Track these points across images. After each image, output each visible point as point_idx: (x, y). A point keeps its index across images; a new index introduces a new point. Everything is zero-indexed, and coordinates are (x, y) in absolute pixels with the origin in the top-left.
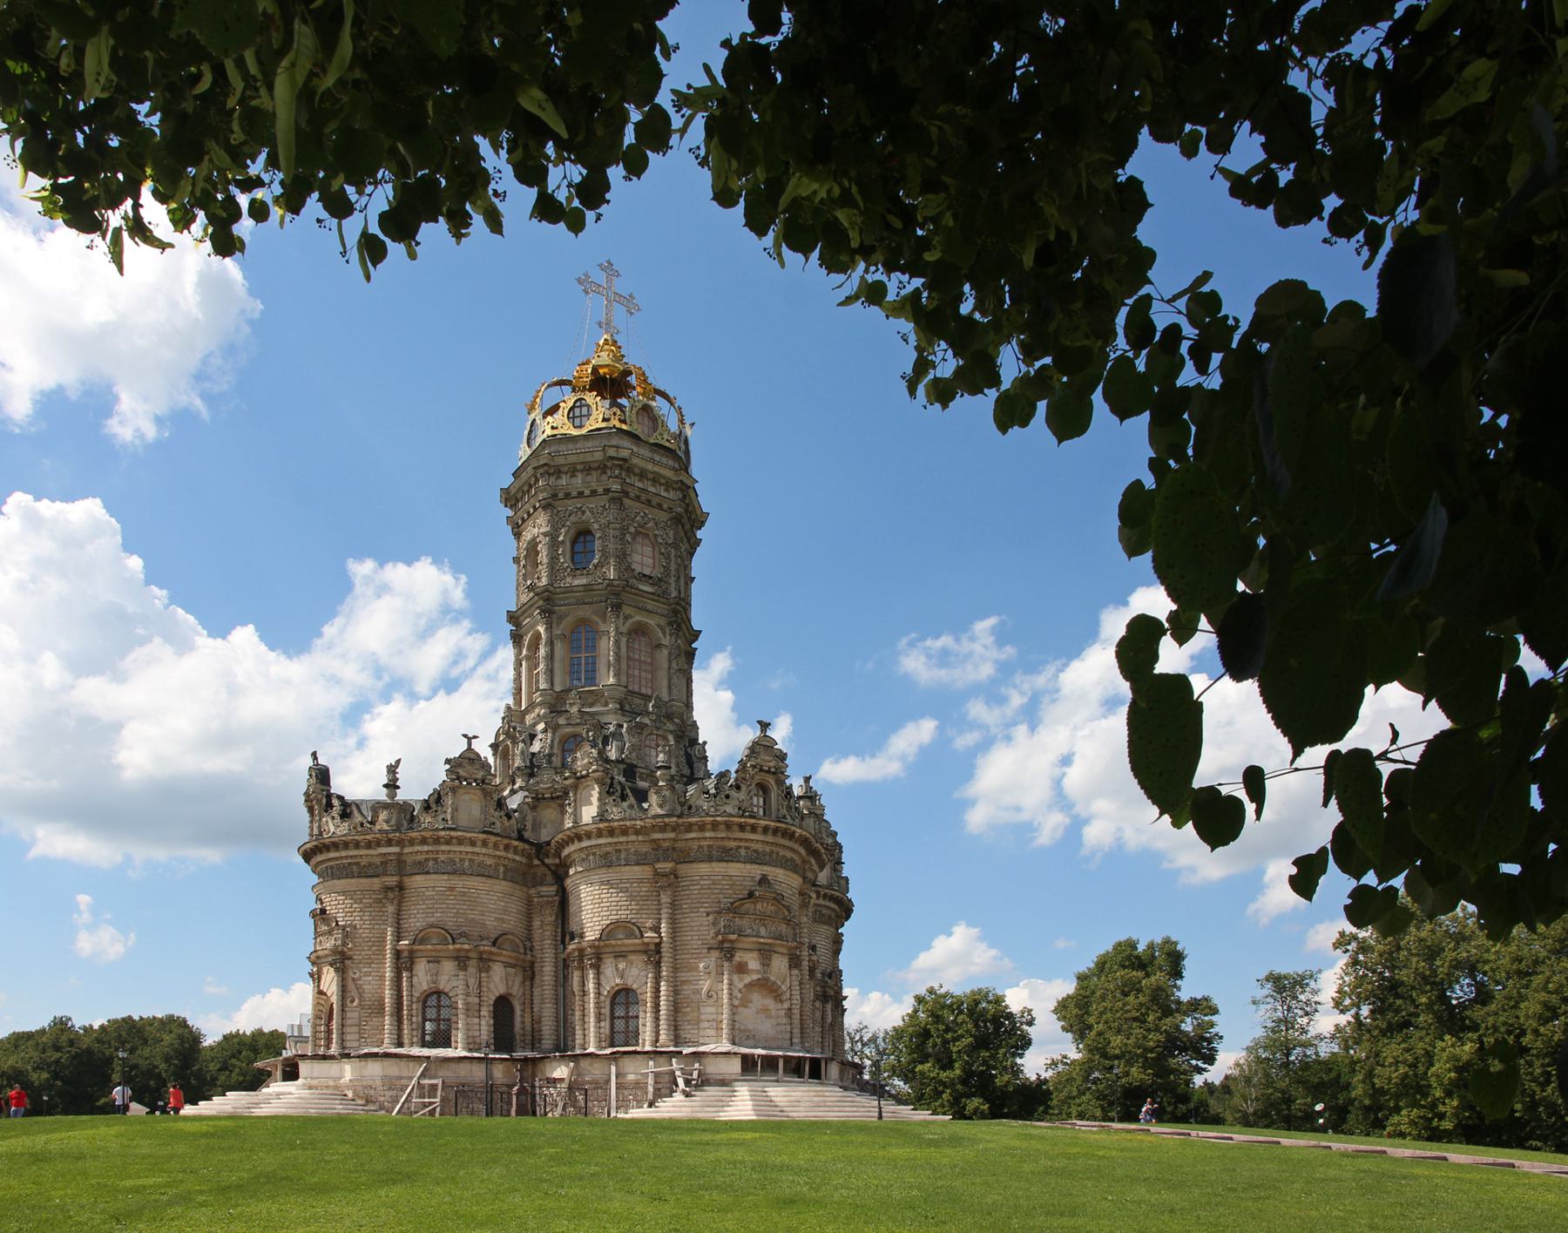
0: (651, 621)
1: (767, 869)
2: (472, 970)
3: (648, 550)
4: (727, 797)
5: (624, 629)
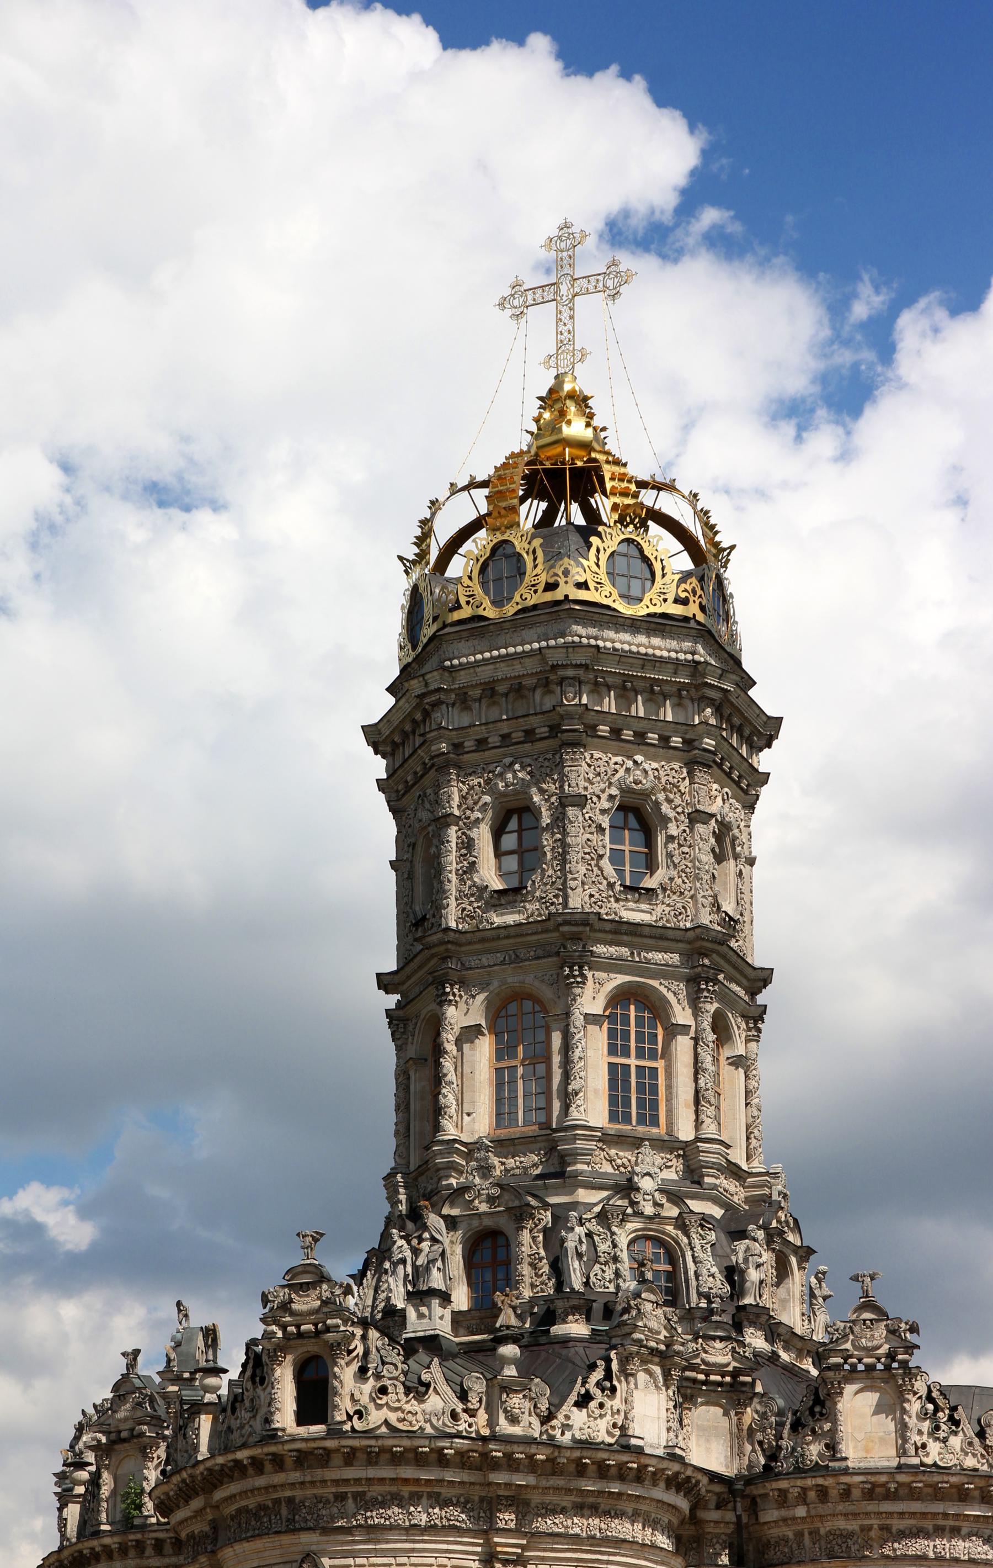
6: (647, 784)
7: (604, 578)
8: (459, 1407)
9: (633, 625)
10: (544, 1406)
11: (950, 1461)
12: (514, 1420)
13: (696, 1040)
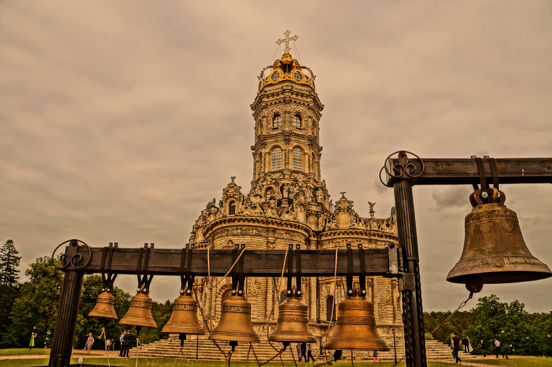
0: (278, 144)
6: (301, 111)
8: (262, 212)
9: (299, 84)
10: (279, 213)
11: (360, 228)
12: (274, 215)
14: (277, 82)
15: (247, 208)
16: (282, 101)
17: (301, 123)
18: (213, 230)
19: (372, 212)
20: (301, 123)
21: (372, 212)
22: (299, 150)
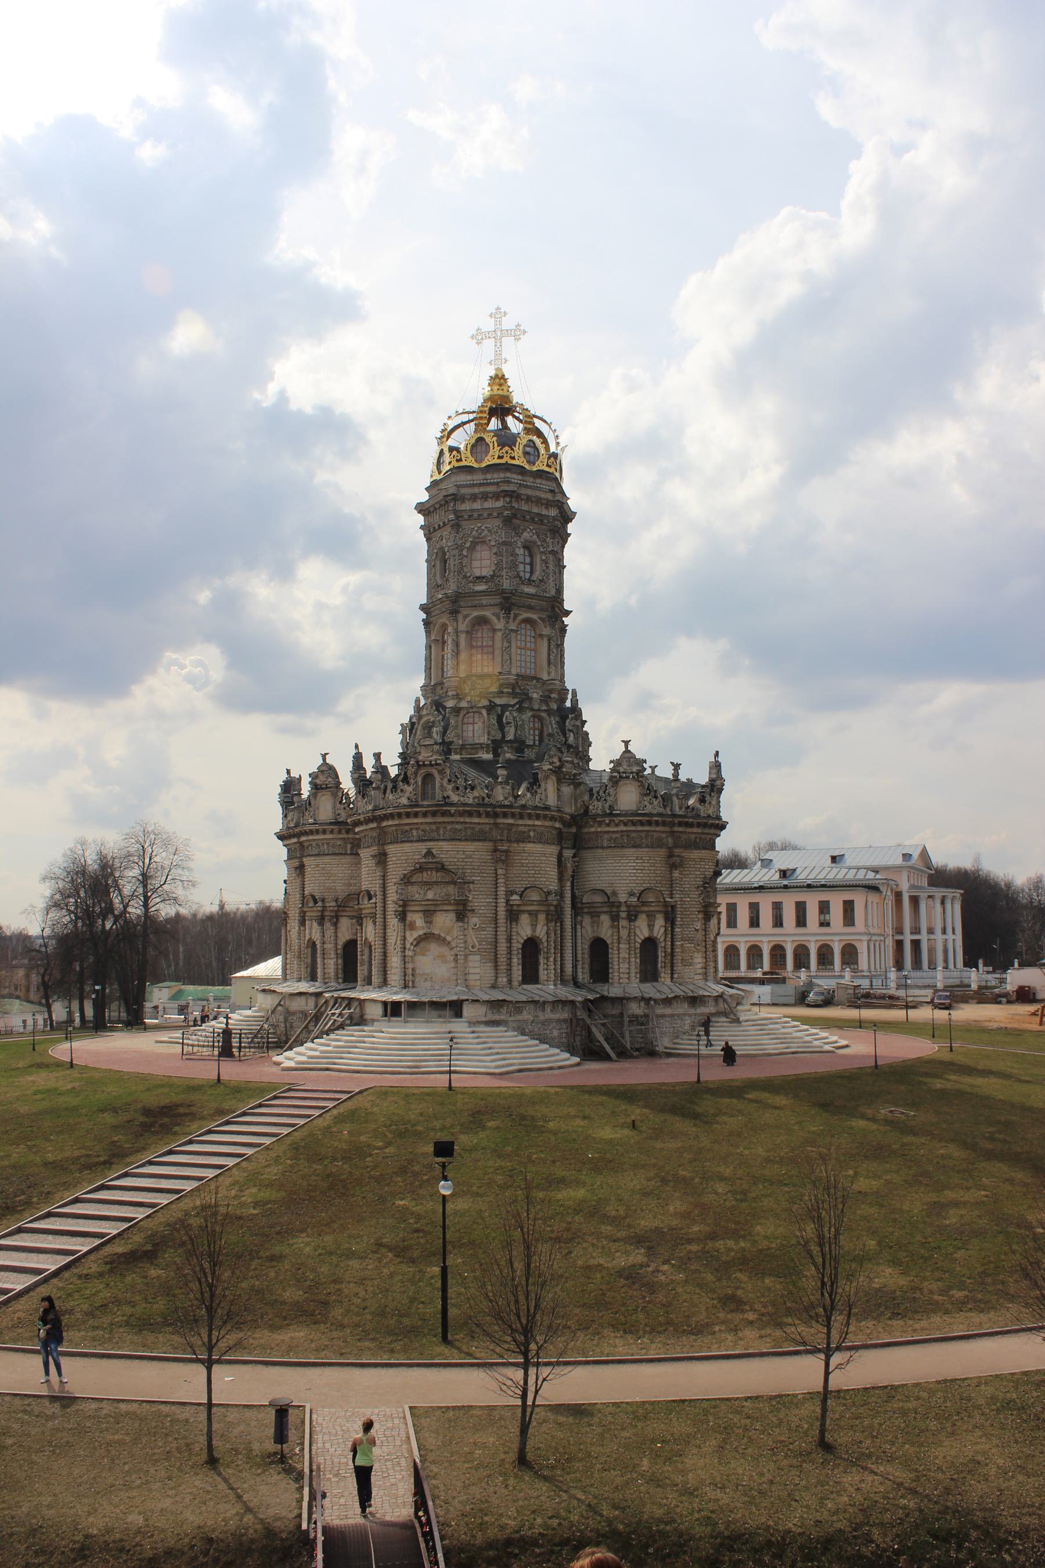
0: (487, 613)
1: (430, 844)
2: (328, 925)
3: (486, 554)
4: (402, 791)
5: (463, 626)
7: (521, 454)
13: (549, 640)
14: (483, 465)
15: (458, 789)
16: (495, 514)
17: (532, 564)
18: (385, 824)
19: (676, 775)
20: (531, 564)
21: (676, 775)
22: (529, 627)
